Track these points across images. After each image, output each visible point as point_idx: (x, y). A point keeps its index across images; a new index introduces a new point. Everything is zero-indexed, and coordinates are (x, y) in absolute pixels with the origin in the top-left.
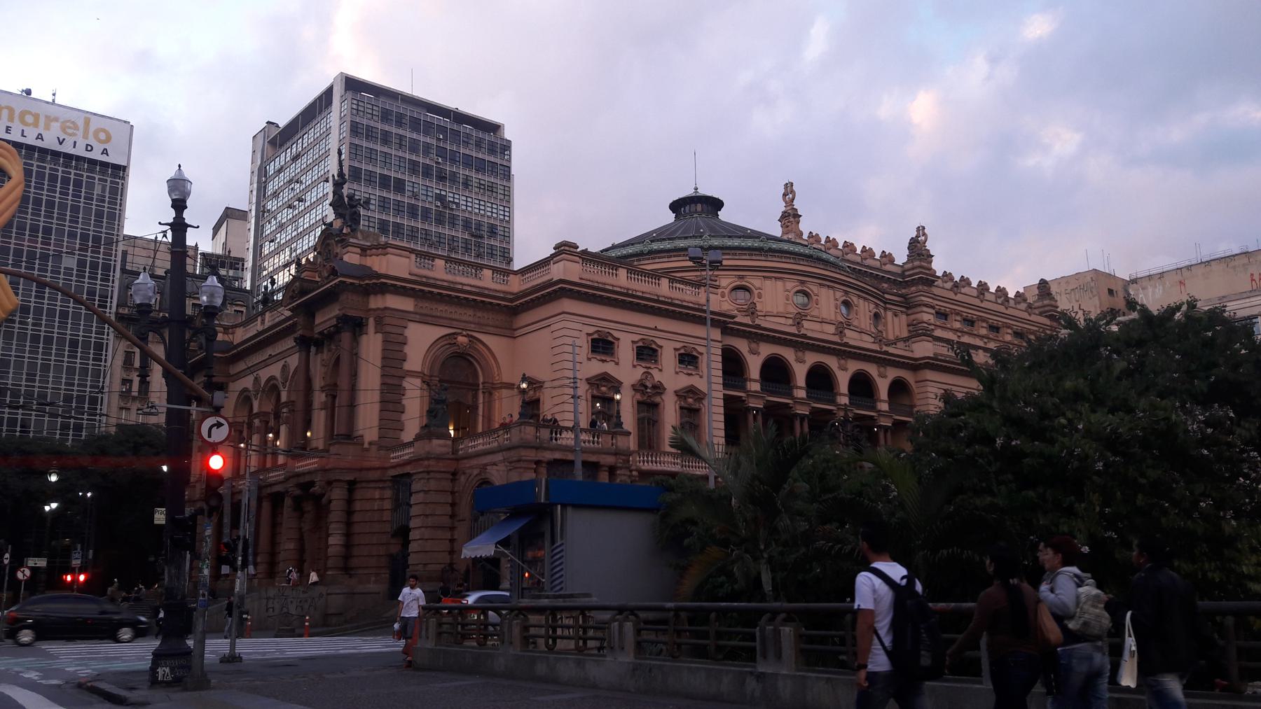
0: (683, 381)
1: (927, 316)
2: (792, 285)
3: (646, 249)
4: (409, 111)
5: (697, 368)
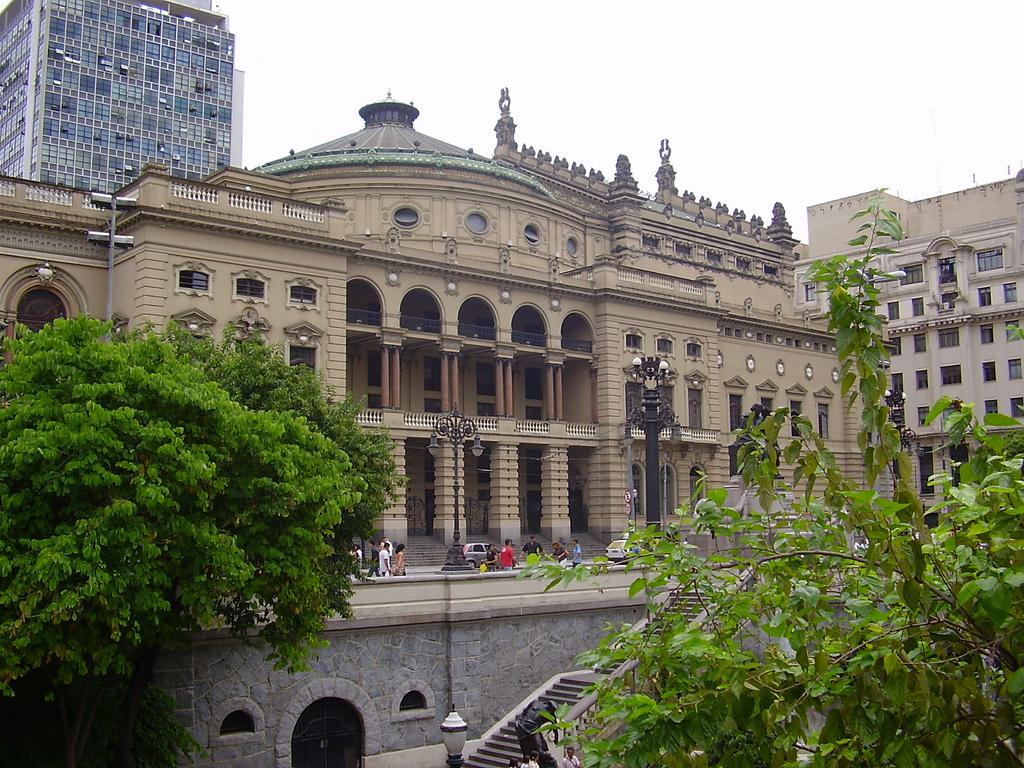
0: (294, 318)
1: (632, 241)
2: (466, 207)
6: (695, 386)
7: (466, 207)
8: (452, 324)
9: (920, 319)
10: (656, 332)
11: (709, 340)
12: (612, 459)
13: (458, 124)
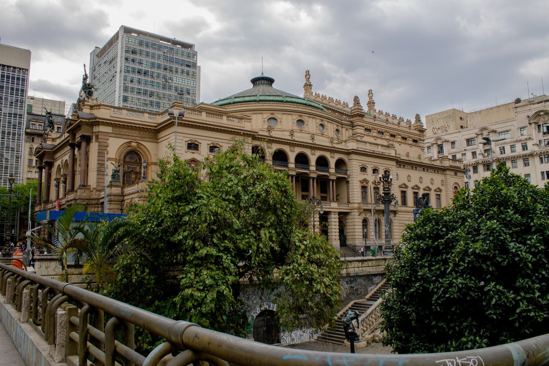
1: (360, 130)
3: (232, 101)
4: (151, 40)
7: (296, 117)
8: (292, 163)
9: (475, 160)
12: (356, 217)
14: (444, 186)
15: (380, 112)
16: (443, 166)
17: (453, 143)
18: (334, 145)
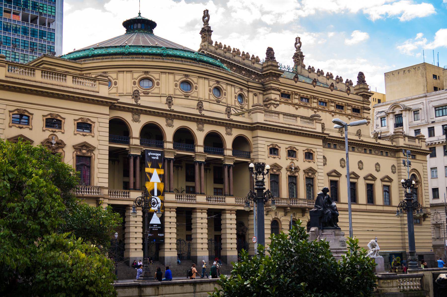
0: (80, 139)
1: (275, 96)
5: (91, 131)
6: (310, 176)
7: (179, 77)
10: (287, 146)
11: (318, 150)
13: (178, 30)
14: (396, 175)
15: (311, 70)
16: (394, 146)
17: (416, 112)
18: (232, 117)
